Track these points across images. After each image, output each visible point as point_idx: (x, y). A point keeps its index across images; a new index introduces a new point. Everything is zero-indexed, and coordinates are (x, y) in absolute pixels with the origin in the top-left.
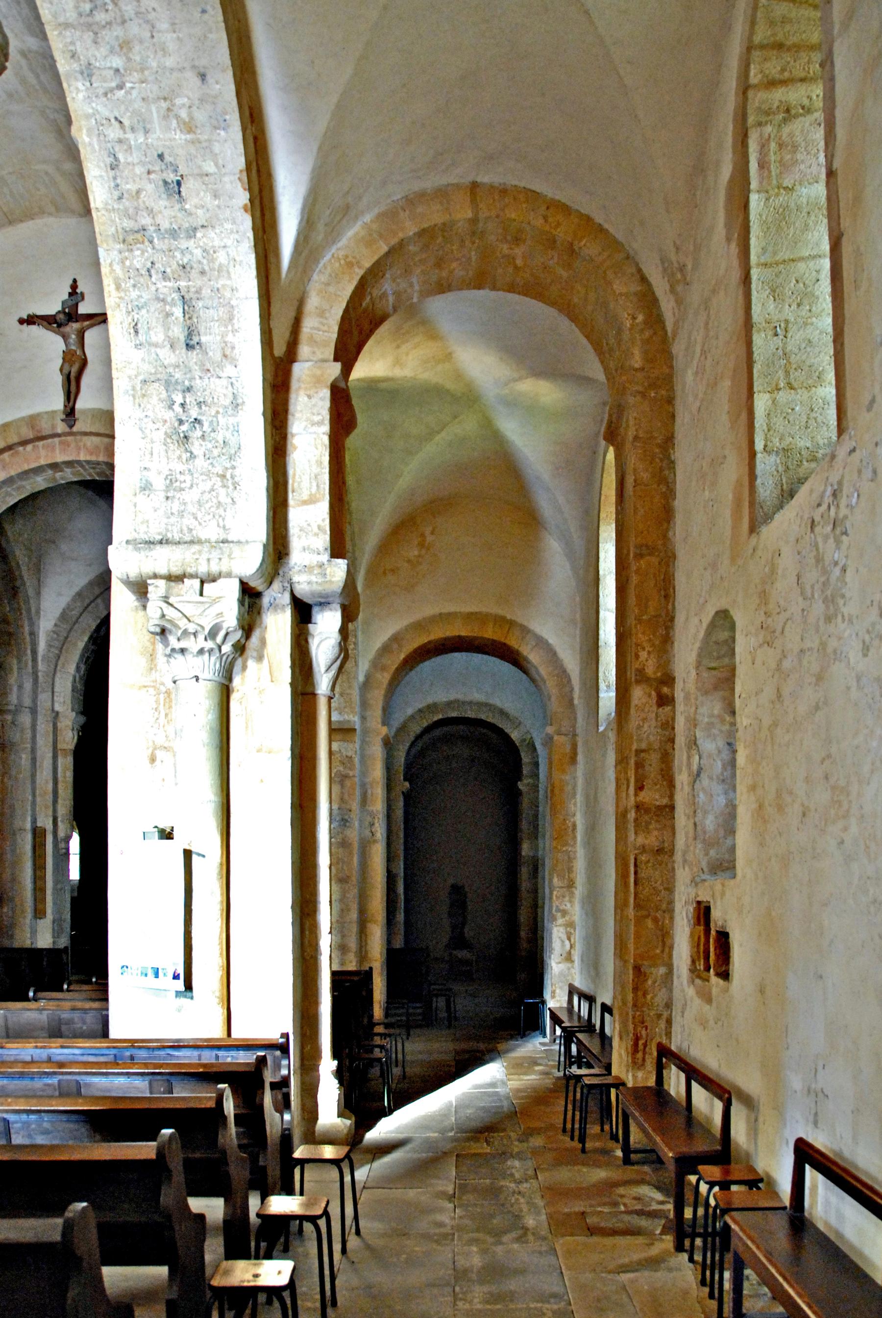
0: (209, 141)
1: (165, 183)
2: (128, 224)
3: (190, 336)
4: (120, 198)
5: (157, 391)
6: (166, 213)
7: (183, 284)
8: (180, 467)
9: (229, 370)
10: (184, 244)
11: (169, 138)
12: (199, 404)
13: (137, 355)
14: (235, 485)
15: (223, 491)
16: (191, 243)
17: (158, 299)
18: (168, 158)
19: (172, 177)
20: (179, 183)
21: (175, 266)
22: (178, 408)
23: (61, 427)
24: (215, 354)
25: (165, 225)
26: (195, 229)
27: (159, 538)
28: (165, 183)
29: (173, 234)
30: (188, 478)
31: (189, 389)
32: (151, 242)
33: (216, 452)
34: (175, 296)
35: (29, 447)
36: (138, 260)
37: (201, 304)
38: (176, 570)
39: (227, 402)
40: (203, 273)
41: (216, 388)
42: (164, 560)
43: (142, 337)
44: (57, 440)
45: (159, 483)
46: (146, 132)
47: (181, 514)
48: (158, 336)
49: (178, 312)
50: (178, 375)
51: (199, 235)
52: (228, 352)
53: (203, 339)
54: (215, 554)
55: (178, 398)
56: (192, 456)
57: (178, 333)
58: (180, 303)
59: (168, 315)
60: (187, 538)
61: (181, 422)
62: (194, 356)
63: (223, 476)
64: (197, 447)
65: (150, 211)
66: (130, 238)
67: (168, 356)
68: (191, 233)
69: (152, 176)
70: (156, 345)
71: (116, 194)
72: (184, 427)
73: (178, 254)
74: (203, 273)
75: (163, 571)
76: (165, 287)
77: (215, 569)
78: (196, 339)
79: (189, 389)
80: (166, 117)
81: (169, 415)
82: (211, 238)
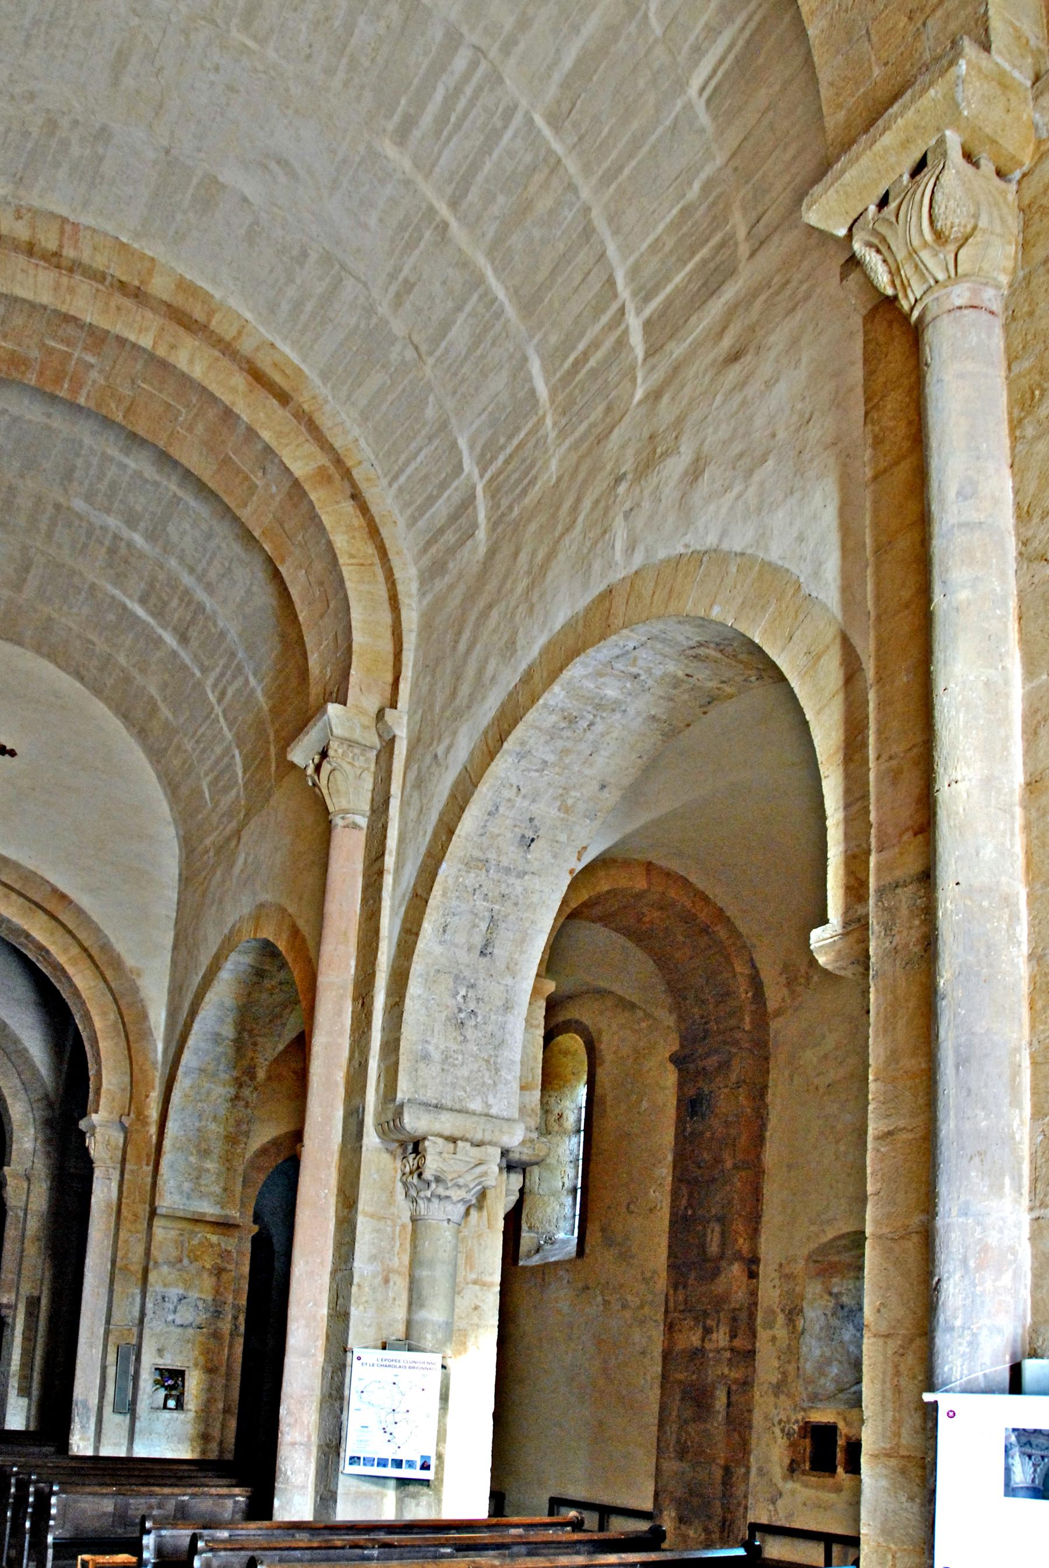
0: (574, 823)
1: (523, 836)
2: (477, 853)
3: (486, 946)
4: (482, 835)
5: (447, 981)
6: (511, 854)
7: (497, 907)
8: (455, 1047)
9: (509, 981)
10: (512, 880)
11: (546, 810)
12: (478, 1000)
13: (438, 949)
14: (497, 1070)
15: (487, 1074)
16: (518, 882)
17: (472, 912)
18: (536, 822)
19: (532, 836)
20: (533, 840)
21: (497, 893)
22: (459, 998)
24: (501, 964)
25: (505, 862)
26: (526, 873)
27: (434, 1102)
28: (523, 836)
29: (508, 871)
30: (460, 1057)
31: (473, 986)
32: (487, 871)
33: (484, 1041)
34: (487, 914)
36: (471, 879)
37: (504, 925)
38: (457, 1134)
39: (500, 1003)
40: (516, 904)
41: (494, 991)
42: (447, 1123)
43: (447, 937)
45: (436, 1056)
46: (534, 801)
47: (453, 1085)
48: (461, 938)
49: (484, 926)
50: (467, 973)
51: (527, 877)
52: (511, 965)
53: (496, 951)
54: (489, 1126)
55: (463, 992)
56: (465, 1040)
57: (478, 941)
58: (488, 920)
59: (475, 926)
60: (457, 1107)
61: (460, 1010)
62: (484, 960)
64: (469, 1033)
65: (499, 850)
66: (472, 864)
67: (463, 956)
68: (522, 874)
69: (517, 829)
70: (456, 946)
71: (481, 831)
72: (462, 1015)
73: (503, 886)
74: (516, 904)
76: (481, 905)
77: (488, 1137)
78: (490, 950)
79: (473, 986)
80: (555, 799)
81: (451, 1002)
82: (536, 883)
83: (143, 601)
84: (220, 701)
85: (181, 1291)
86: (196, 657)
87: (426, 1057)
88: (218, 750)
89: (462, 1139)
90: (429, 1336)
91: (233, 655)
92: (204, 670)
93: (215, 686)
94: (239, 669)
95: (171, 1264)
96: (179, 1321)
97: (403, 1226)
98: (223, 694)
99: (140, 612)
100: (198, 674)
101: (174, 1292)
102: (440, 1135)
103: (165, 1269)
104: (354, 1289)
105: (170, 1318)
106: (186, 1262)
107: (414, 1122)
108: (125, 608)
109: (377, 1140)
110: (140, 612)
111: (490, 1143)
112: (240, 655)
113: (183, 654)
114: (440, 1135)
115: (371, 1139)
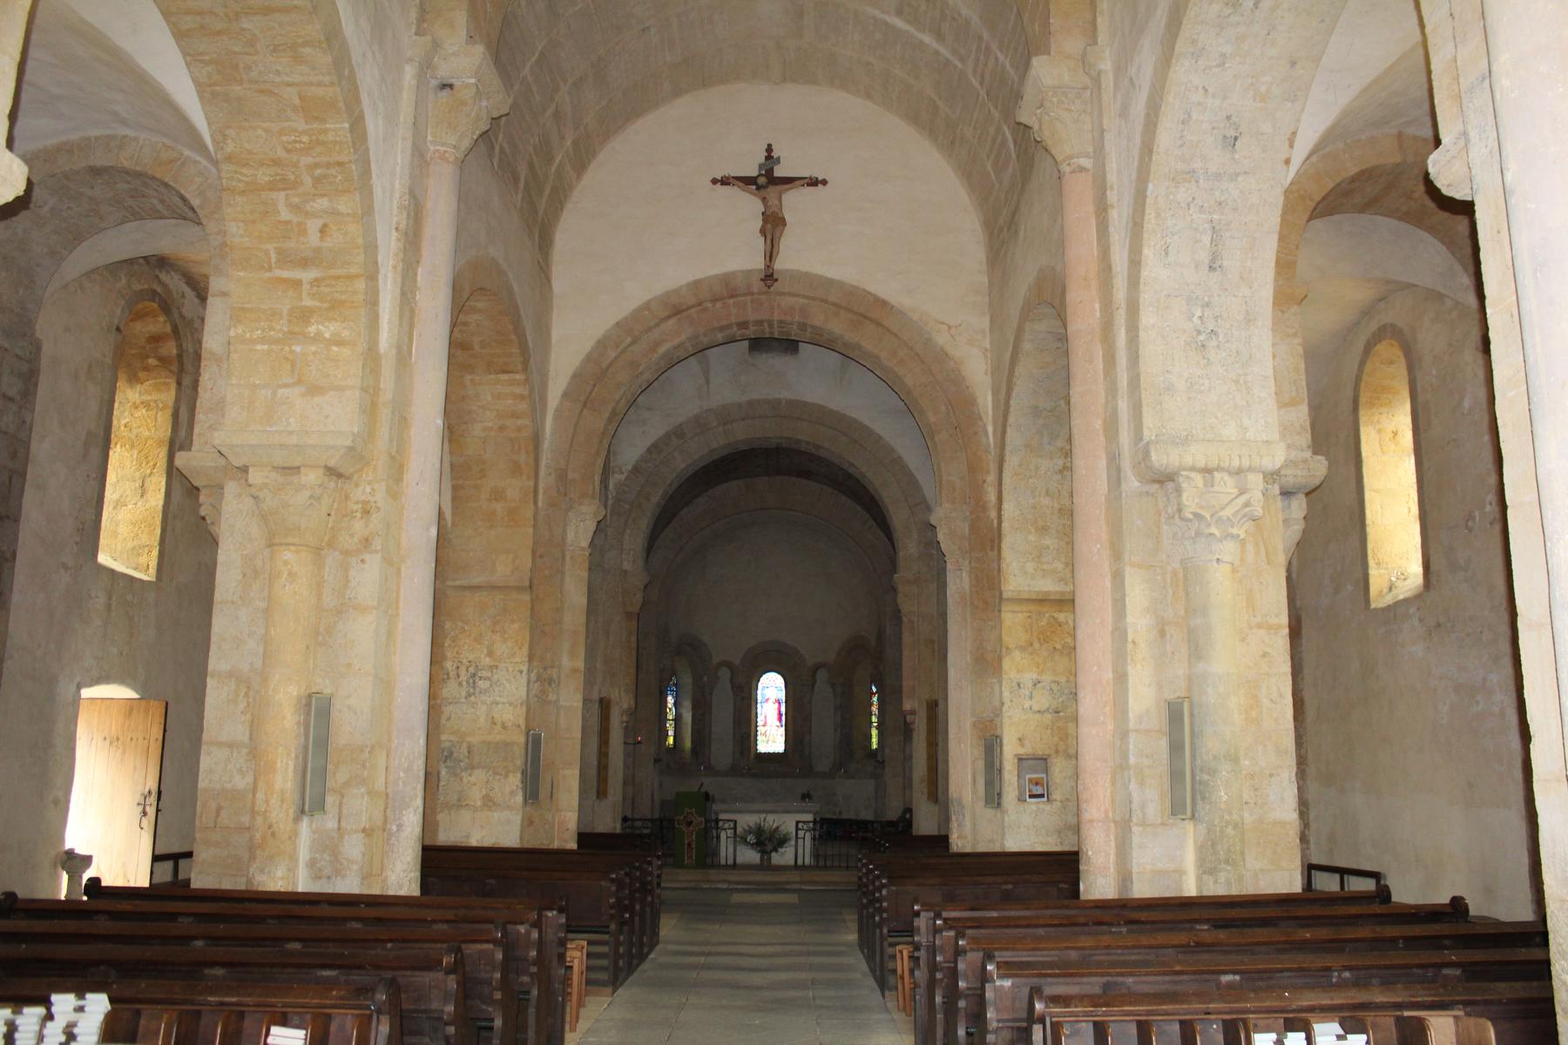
23: (757, 286)
35: (719, 305)
44: (748, 298)
63: (1237, 382)
75: (1201, 464)
83: (899, 13)
84: (981, 84)
85: (1035, 676)
86: (954, 52)
87: (1169, 388)
88: (992, 131)
89: (1219, 469)
90: (1210, 691)
91: (980, 38)
92: (962, 60)
93: (975, 72)
94: (988, 49)
95: (1022, 648)
96: (1036, 708)
97: (1175, 573)
98: (983, 77)
99: (899, 23)
100: (959, 65)
101: (1029, 677)
102: (1193, 469)
103: (1017, 654)
104: (1130, 646)
105: (1027, 705)
106: (1036, 645)
107: (1162, 458)
108: (886, 23)
109: (1137, 484)
110: (899, 23)
111: (1250, 469)
112: (986, 36)
113: (942, 50)
114: (1193, 469)
115: (1132, 483)
